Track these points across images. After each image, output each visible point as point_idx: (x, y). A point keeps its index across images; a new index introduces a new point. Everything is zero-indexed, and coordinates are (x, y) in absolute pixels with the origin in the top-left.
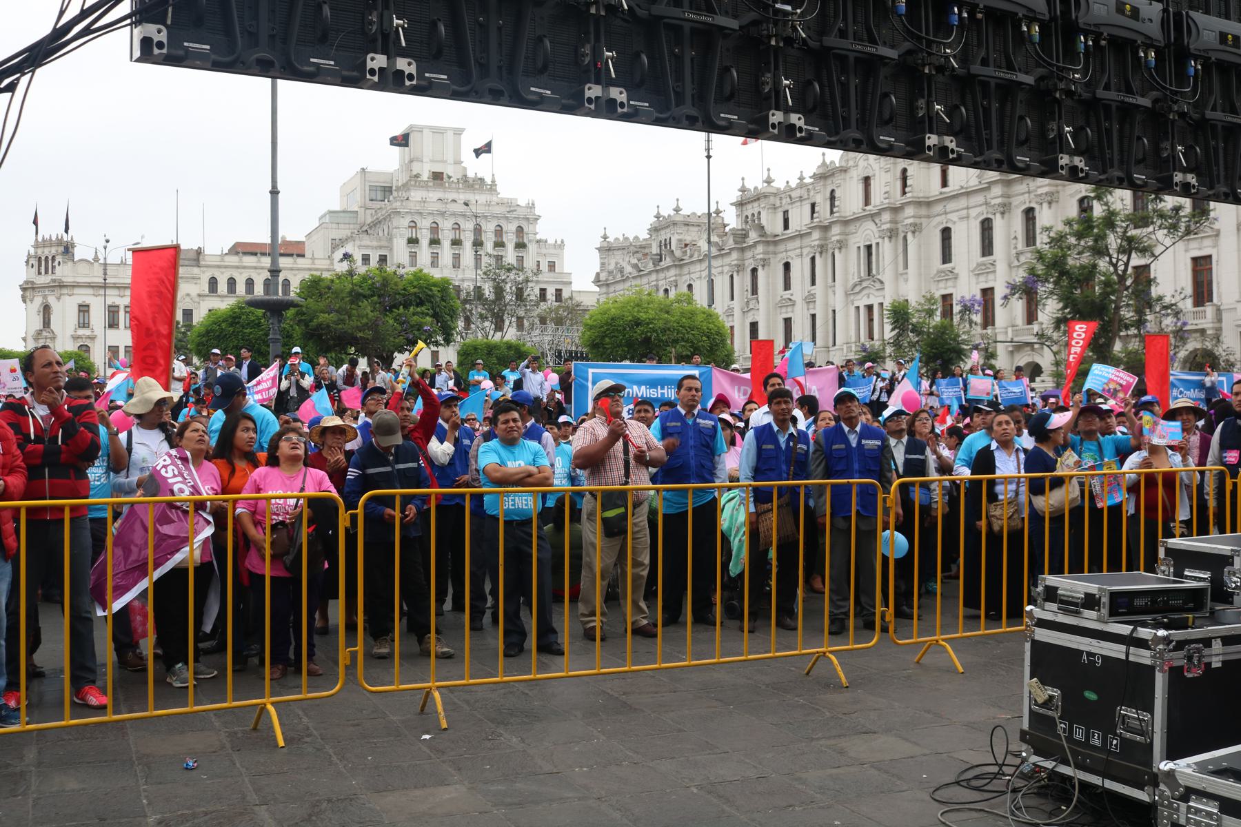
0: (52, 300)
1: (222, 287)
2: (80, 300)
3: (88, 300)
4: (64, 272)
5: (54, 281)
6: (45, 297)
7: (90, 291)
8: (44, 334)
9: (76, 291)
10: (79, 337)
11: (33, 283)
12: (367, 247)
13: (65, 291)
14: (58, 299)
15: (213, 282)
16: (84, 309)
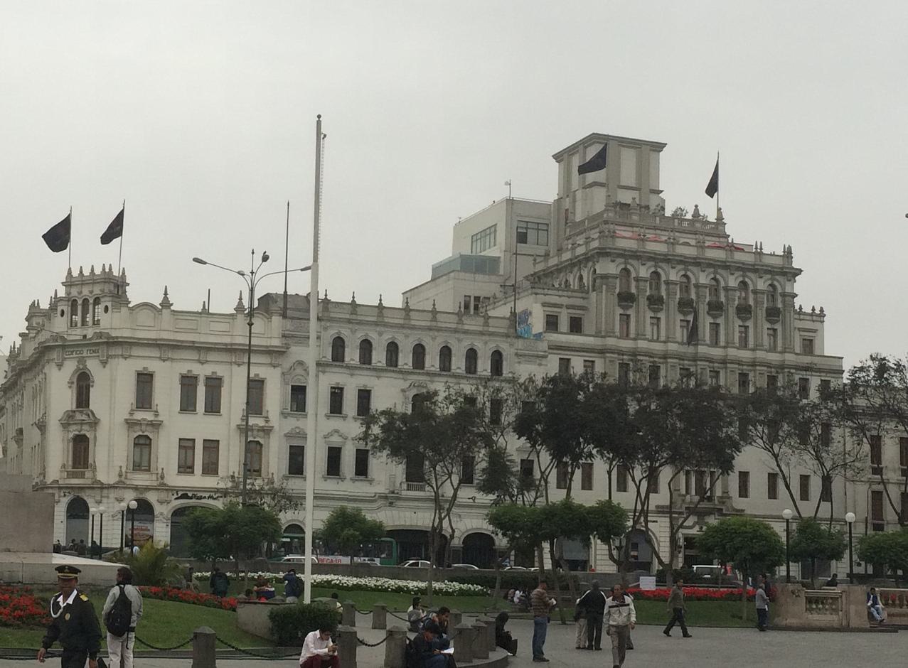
0: (93, 365)
1: (352, 355)
2: (140, 365)
3: (153, 366)
4: (111, 322)
5: (100, 335)
6: (82, 361)
7: (156, 353)
8: (79, 417)
9: (136, 351)
10: (138, 423)
11: (63, 339)
12: (555, 305)
13: (118, 351)
14: (104, 363)
15: (339, 344)
16: (145, 381)
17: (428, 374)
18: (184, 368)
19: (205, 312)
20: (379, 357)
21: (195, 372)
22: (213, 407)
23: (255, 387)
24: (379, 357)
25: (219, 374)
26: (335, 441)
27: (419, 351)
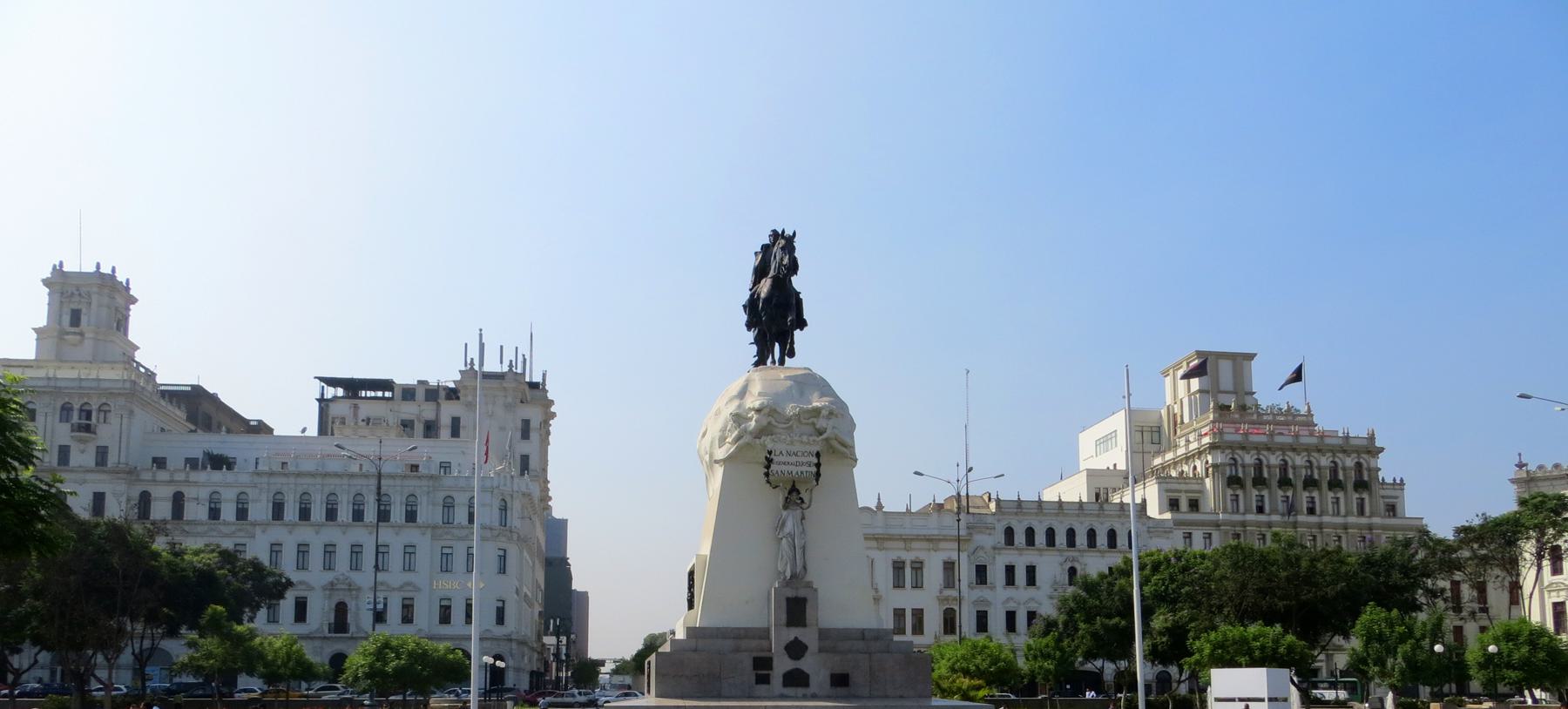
1: (1020, 538)
15: (1009, 533)
18: (894, 555)
19: (909, 511)
20: (1040, 539)
22: (918, 585)
23: (949, 567)
24: (1040, 539)
26: (1011, 606)
27: (1071, 534)
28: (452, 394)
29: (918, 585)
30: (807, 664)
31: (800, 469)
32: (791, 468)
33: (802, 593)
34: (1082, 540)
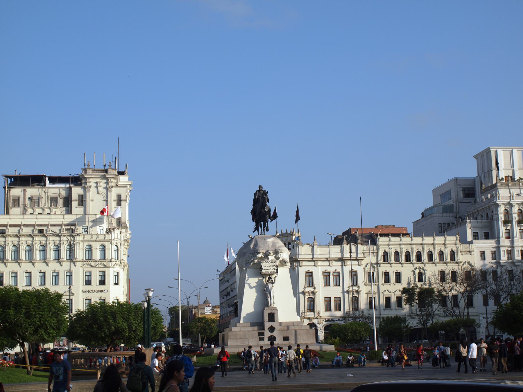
1: (392, 258)
9: (304, 263)
16: (310, 275)
17: (423, 263)
21: (328, 271)
24: (403, 258)
25: (338, 270)
26: (387, 294)
28: (77, 180)
29: (337, 284)
30: (275, 334)
31: (271, 271)
32: (268, 271)
33: (273, 312)
34: (425, 257)
